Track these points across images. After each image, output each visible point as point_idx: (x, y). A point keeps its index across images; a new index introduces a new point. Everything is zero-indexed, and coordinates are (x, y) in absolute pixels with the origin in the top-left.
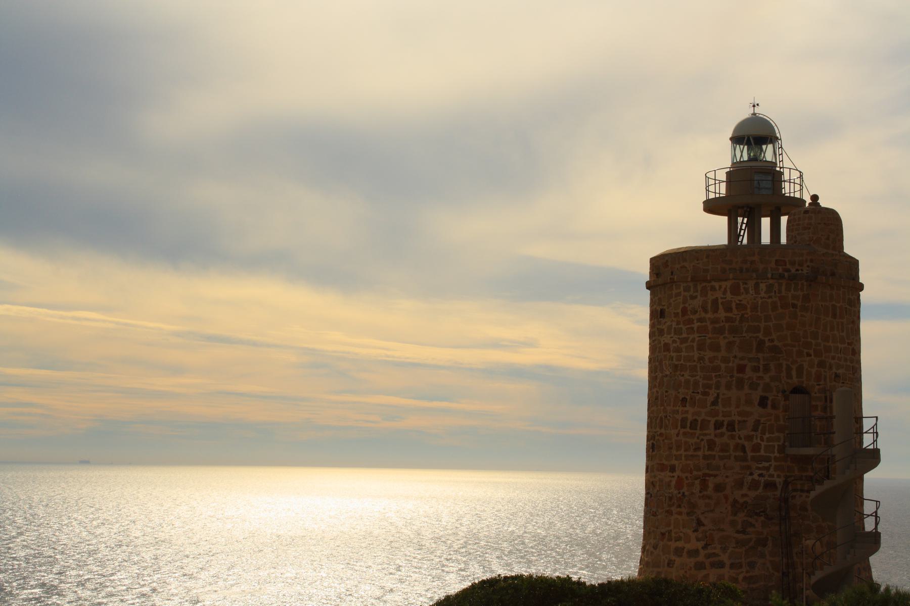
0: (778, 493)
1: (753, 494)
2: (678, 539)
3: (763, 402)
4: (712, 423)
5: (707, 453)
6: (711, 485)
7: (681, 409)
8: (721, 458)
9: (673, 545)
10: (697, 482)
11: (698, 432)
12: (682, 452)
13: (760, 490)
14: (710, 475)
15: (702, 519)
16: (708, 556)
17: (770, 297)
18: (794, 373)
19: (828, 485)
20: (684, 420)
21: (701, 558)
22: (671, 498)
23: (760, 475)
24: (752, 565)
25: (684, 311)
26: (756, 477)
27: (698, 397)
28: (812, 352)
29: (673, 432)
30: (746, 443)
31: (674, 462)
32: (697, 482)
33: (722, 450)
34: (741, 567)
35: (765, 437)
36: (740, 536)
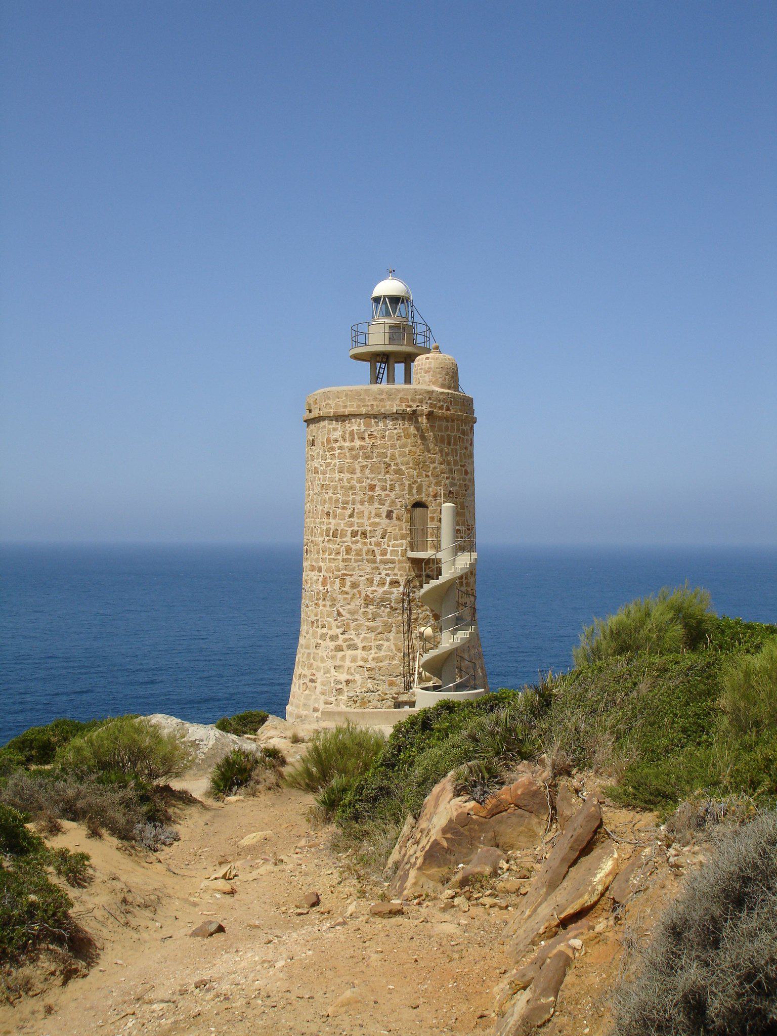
0: (401, 589)
1: (381, 590)
2: (323, 627)
3: (389, 515)
4: (349, 532)
5: (345, 557)
6: (348, 584)
7: (326, 520)
8: (356, 561)
9: (320, 631)
10: (337, 580)
11: (339, 540)
12: (326, 556)
13: (386, 587)
14: (347, 575)
15: (341, 610)
16: (345, 640)
17: (395, 429)
18: (414, 491)
19: (433, 583)
20: (328, 530)
21: (340, 642)
22: (318, 593)
23: (387, 575)
24: (379, 647)
25: (329, 441)
26: (383, 575)
27: (339, 511)
28: (430, 474)
29: (321, 539)
30: (375, 549)
31: (321, 564)
32: (337, 580)
33: (358, 555)
34: (371, 649)
35: (390, 544)
36: (372, 624)
